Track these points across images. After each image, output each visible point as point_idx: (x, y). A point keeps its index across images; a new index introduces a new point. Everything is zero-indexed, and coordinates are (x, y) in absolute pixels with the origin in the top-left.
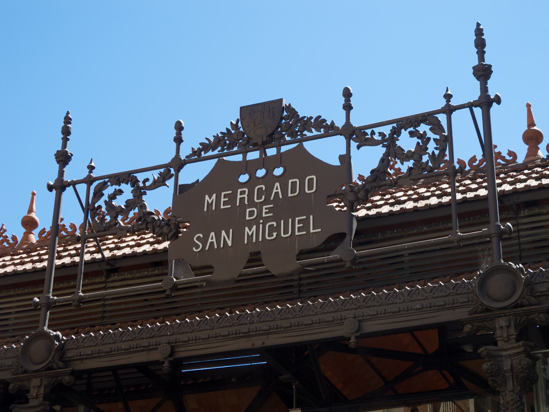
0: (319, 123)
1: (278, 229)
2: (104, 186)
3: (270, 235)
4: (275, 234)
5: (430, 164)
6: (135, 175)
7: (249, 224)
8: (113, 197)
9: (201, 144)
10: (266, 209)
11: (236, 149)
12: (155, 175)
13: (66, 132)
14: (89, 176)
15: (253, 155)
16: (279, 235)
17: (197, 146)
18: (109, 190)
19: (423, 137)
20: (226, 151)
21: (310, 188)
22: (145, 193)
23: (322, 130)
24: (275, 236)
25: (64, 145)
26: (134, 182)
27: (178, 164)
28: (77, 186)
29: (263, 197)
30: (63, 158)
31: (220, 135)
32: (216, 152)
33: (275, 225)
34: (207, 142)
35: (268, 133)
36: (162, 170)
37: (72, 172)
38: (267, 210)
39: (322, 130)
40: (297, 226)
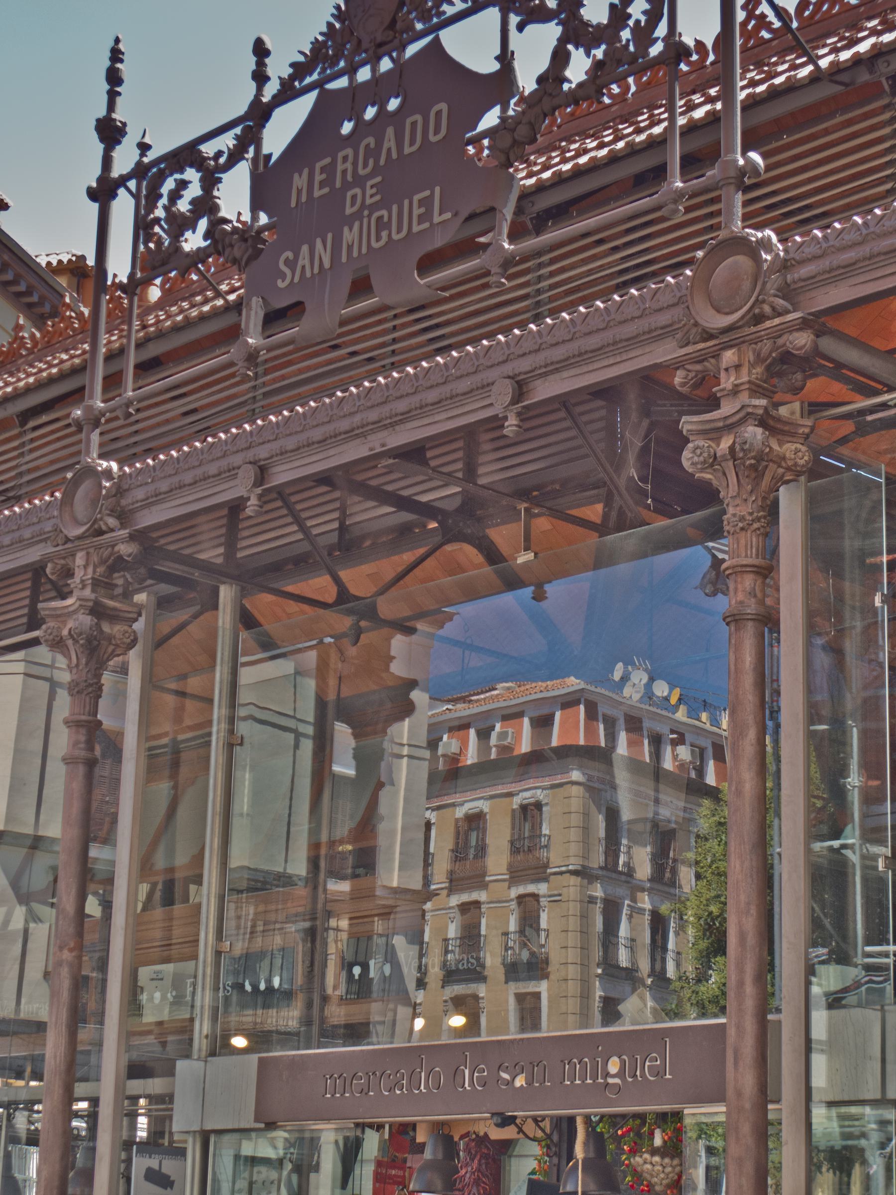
2: (161, 178)
5: (632, 48)
8: (175, 196)
9: (292, 65)
12: (227, 141)
13: (114, 78)
14: (139, 164)
17: (287, 72)
18: (169, 184)
20: (328, 71)
25: (111, 106)
30: (110, 132)
31: (320, 38)
32: (315, 76)
34: (302, 59)
35: (386, 23)
37: (125, 159)
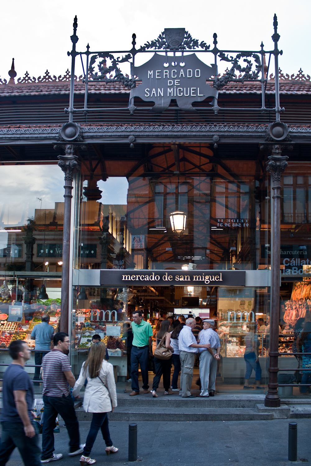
0: (203, 45)
1: (183, 92)
3: (180, 94)
4: (182, 94)
6: (112, 54)
7: (170, 87)
9: (145, 44)
10: (177, 81)
11: (162, 49)
15: (171, 54)
16: (183, 94)
19: (249, 62)
21: (198, 75)
22: (118, 64)
23: (204, 48)
24: (182, 95)
26: (112, 57)
27: (134, 51)
28: (82, 55)
29: (176, 75)
30: (74, 39)
31: (154, 41)
33: (182, 90)
34: (148, 44)
36: (127, 54)
38: (178, 83)
39: (204, 48)
40: (192, 92)
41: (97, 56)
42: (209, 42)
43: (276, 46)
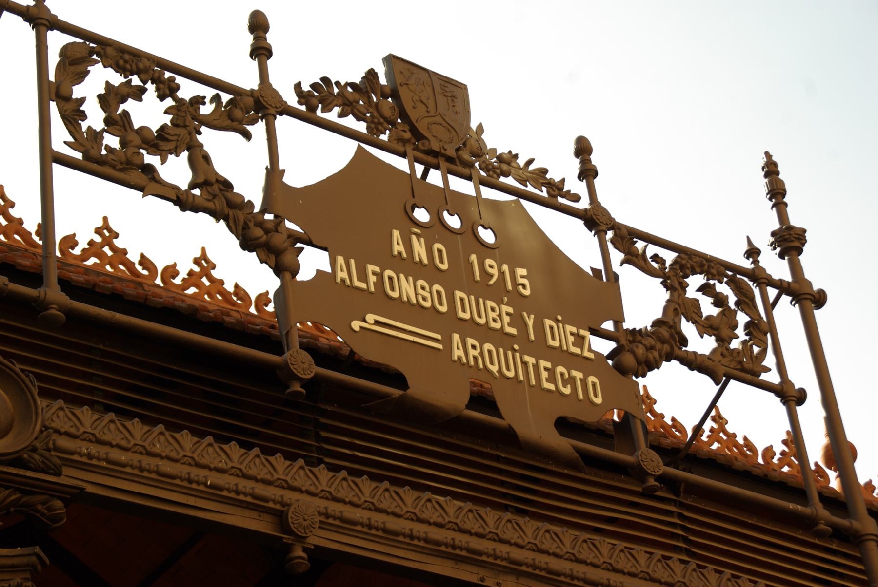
19: (720, 301)
41: (92, 51)
42: (564, 169)
43: (796, 269)
